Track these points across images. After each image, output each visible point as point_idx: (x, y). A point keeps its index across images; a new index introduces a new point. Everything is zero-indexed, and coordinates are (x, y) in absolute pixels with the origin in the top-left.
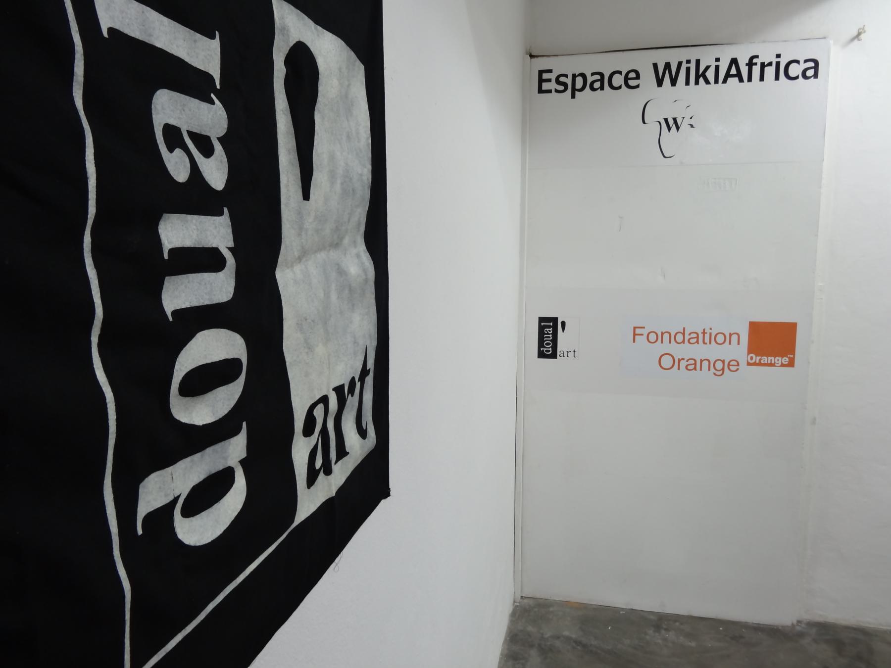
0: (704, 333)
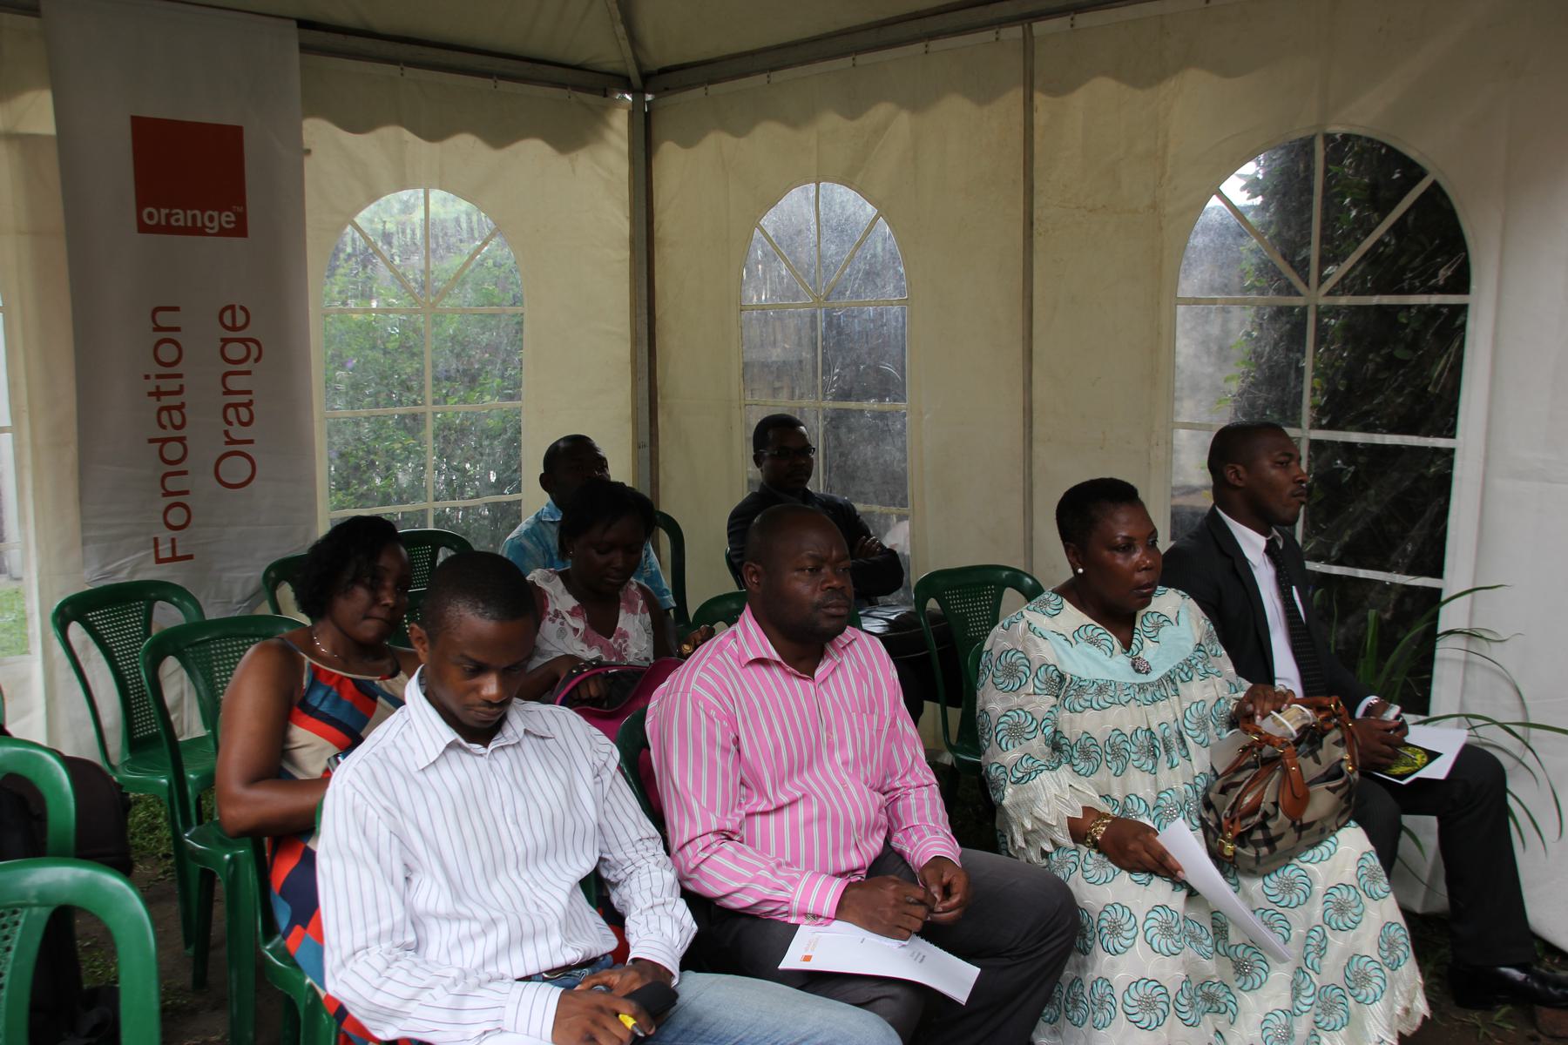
0: (158, 394)
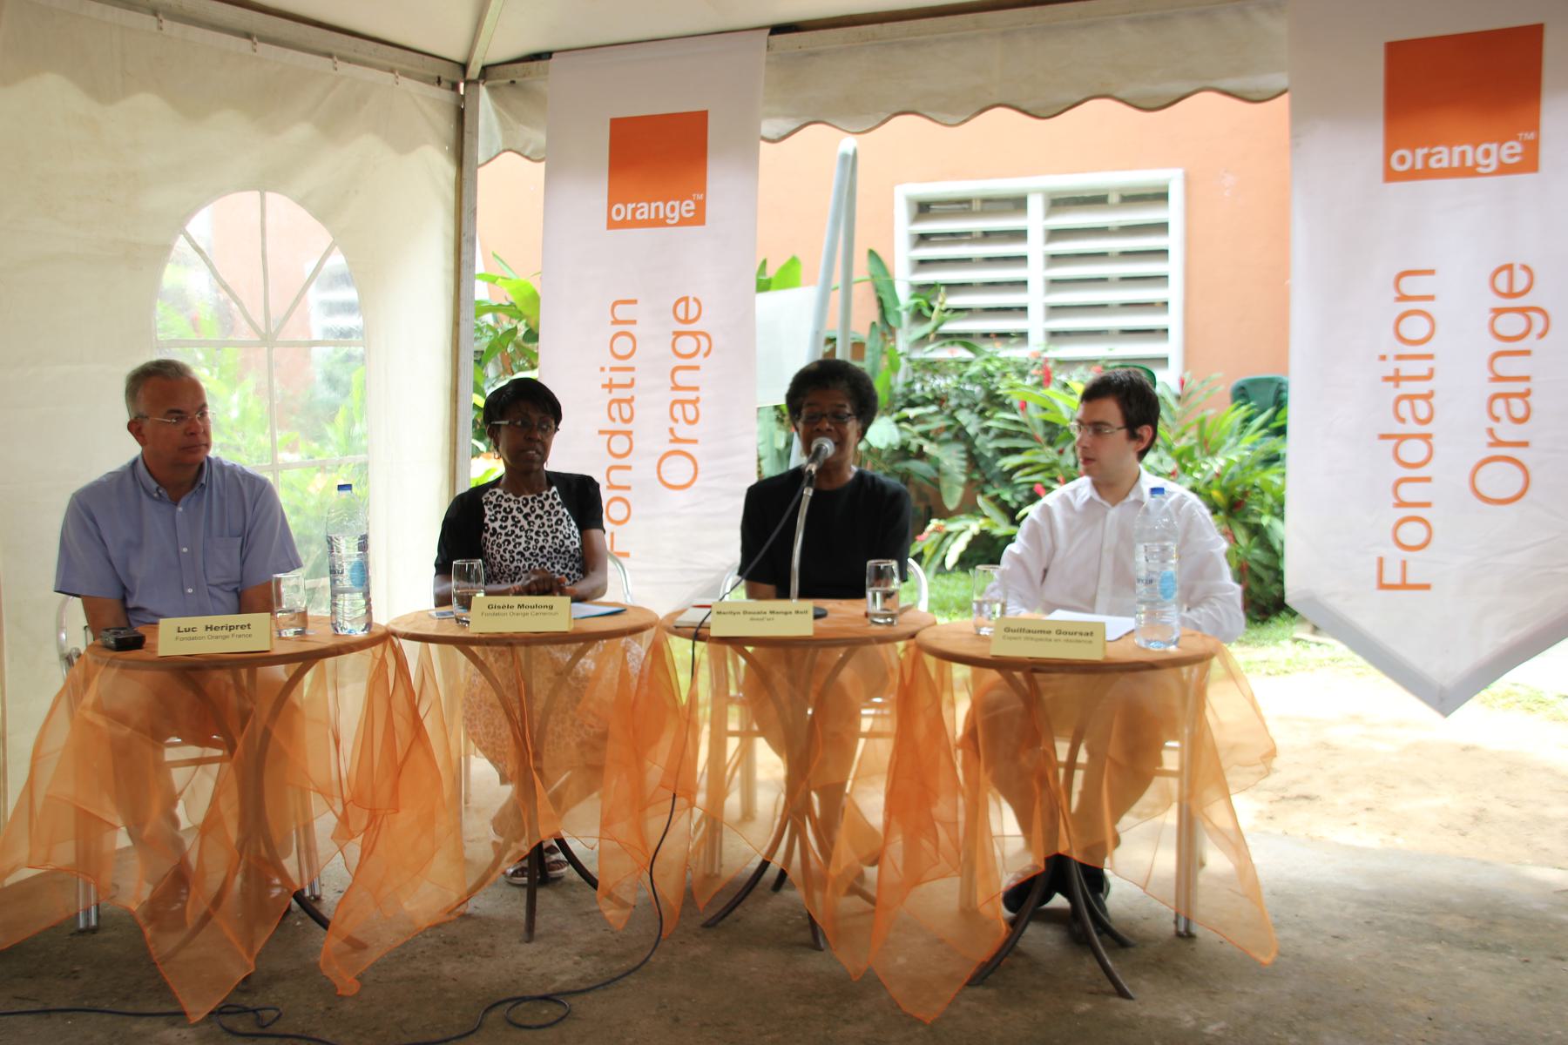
0: (610, 386)
